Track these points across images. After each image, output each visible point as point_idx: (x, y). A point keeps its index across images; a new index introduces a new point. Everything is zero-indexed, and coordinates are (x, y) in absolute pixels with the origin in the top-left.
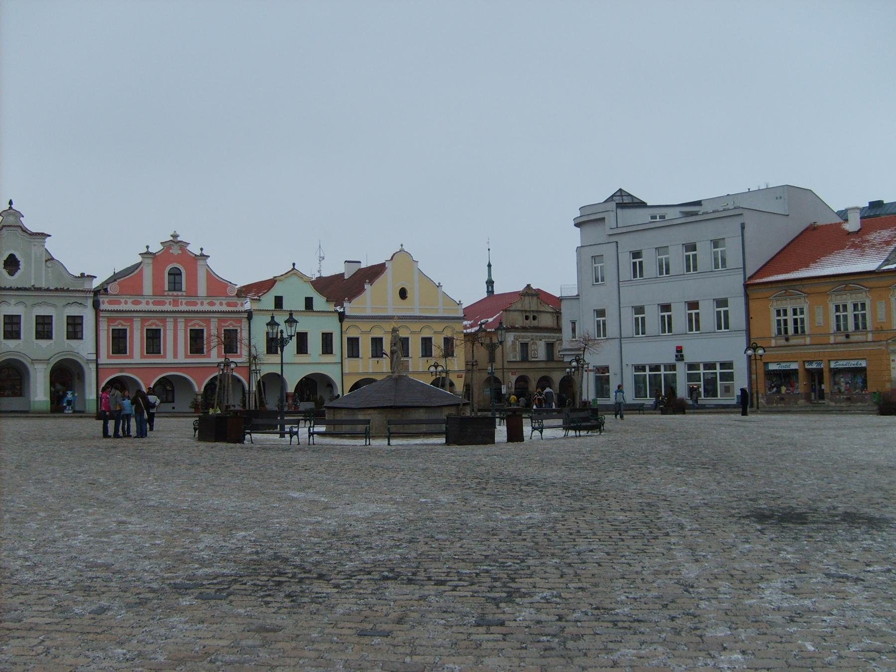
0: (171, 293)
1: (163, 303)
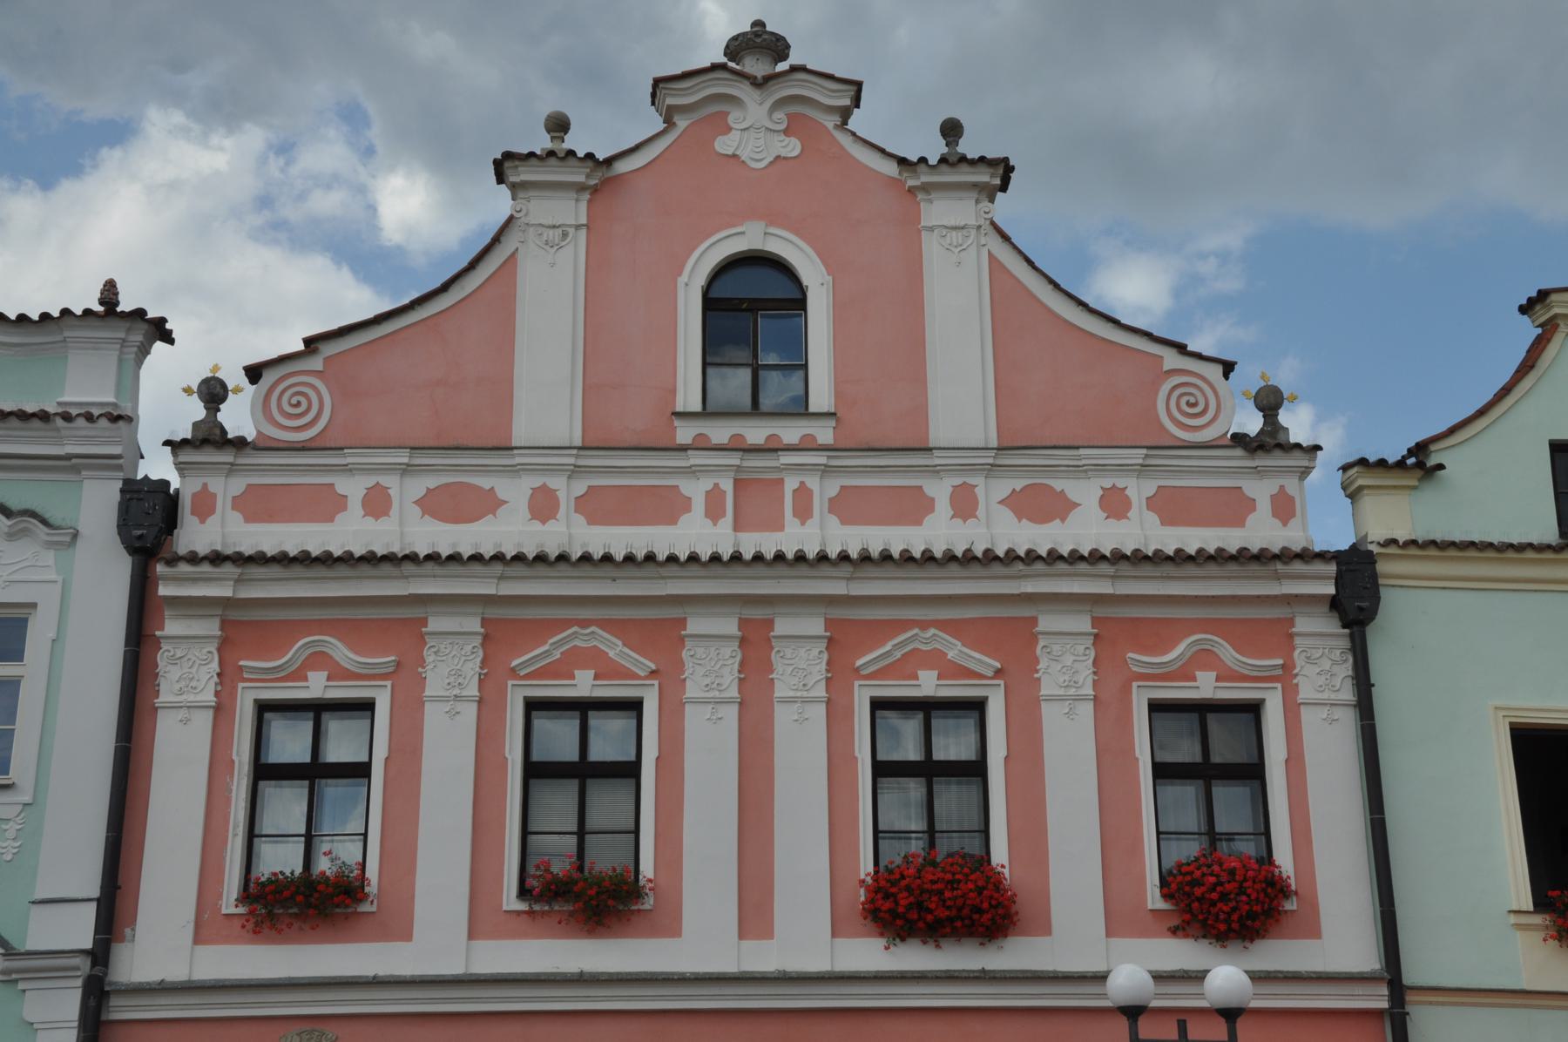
0: (720, 432)
1: (669, 507)
